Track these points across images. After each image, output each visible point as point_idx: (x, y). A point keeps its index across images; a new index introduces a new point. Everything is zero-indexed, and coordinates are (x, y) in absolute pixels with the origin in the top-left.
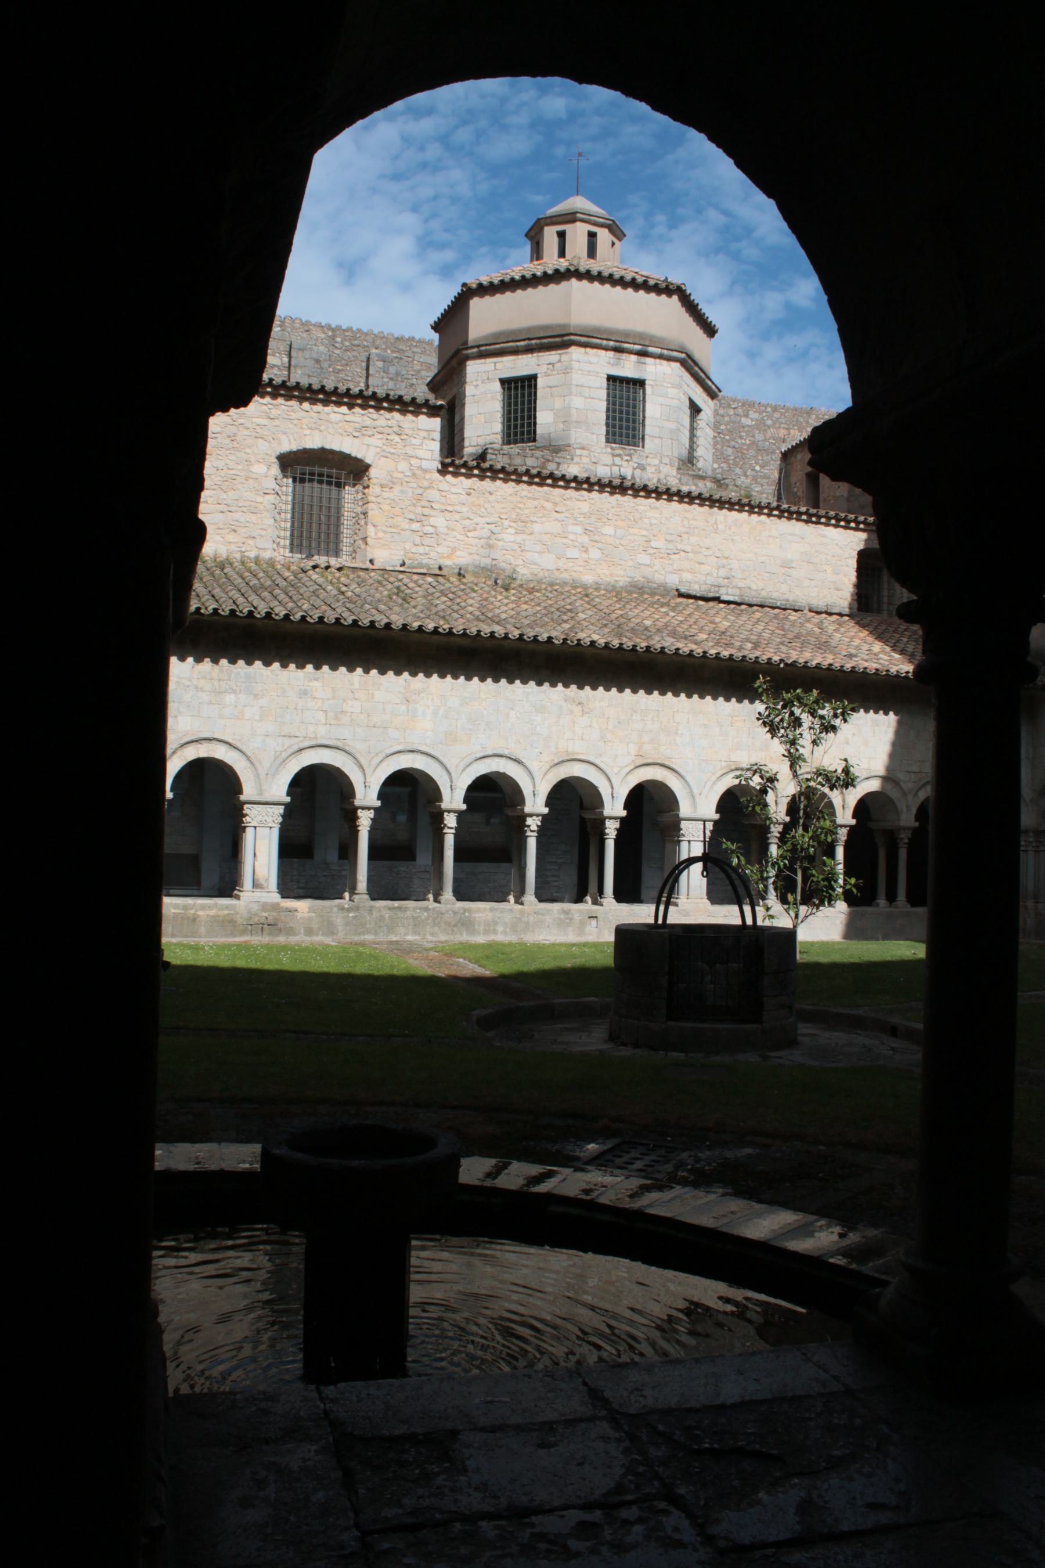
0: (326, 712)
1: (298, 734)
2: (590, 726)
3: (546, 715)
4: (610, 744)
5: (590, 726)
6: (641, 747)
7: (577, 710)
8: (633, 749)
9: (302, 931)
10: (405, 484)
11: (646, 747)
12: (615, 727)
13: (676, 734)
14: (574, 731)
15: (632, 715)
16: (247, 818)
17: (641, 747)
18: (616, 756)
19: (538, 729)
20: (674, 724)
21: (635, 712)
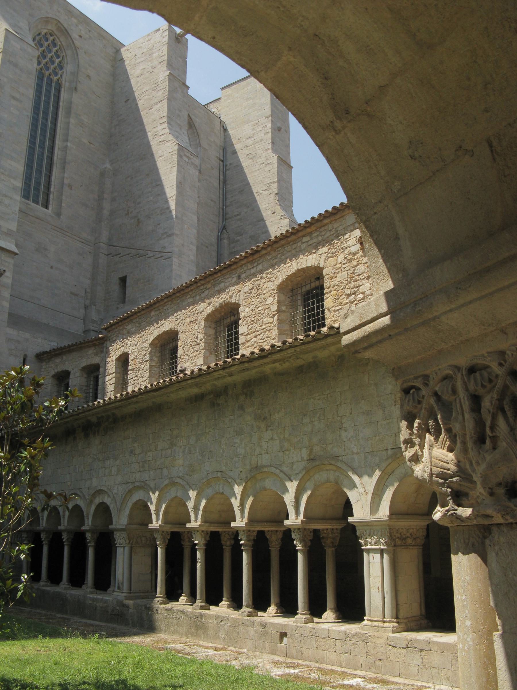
0: (139, 463)
1: (129, 481)
2: (272, 439)
3: (243, 436)
4: (287, 453)
5: (272, 439)
6: (311, 450)
7: (263, 425)
8: (305, 453)
9: (131, 622)
10: (343, 270)
11: (316, 449)
12: (290, 434)
13: (341, 428)
14: (261, 446)
15: (302, 419)
16: (309, 539)
17: (311, 450)
18: (292, 463)
19: (238, 449)
20: (339, 418)
21: (305, 415)
